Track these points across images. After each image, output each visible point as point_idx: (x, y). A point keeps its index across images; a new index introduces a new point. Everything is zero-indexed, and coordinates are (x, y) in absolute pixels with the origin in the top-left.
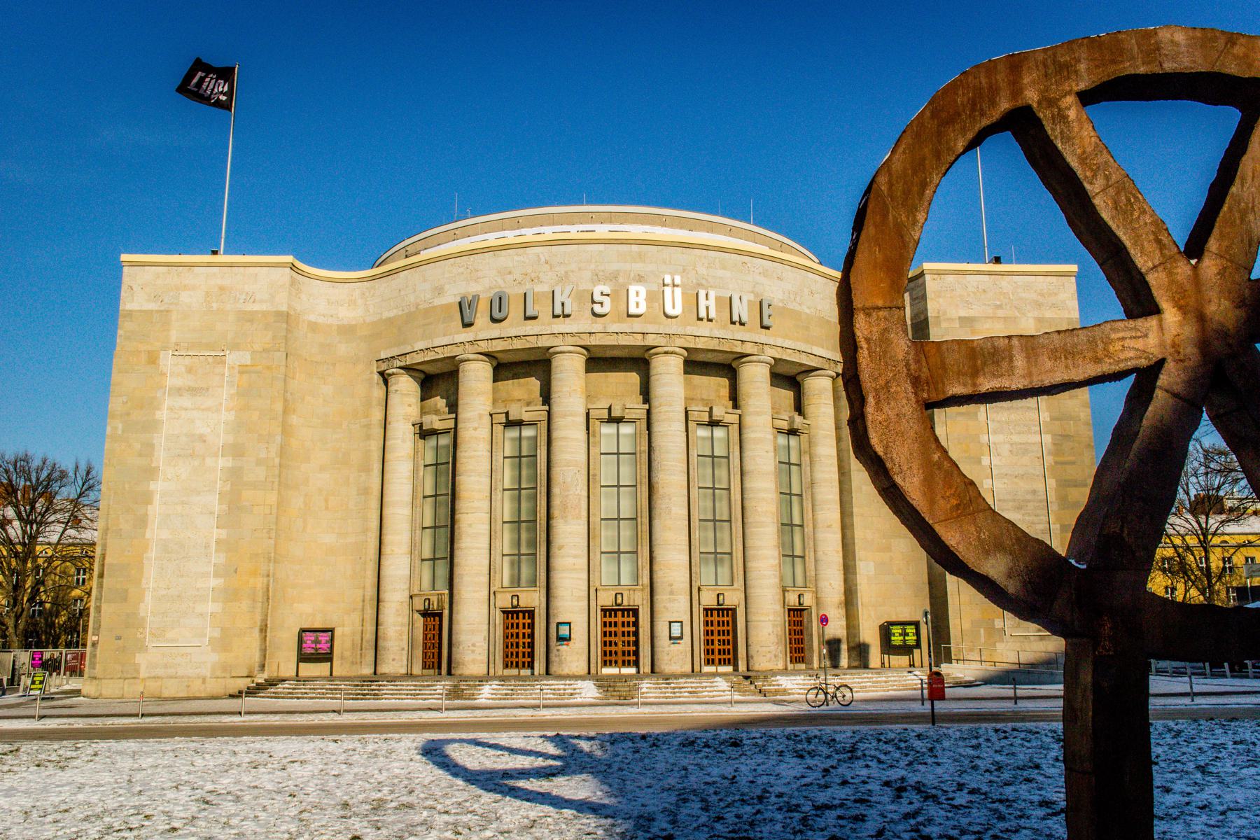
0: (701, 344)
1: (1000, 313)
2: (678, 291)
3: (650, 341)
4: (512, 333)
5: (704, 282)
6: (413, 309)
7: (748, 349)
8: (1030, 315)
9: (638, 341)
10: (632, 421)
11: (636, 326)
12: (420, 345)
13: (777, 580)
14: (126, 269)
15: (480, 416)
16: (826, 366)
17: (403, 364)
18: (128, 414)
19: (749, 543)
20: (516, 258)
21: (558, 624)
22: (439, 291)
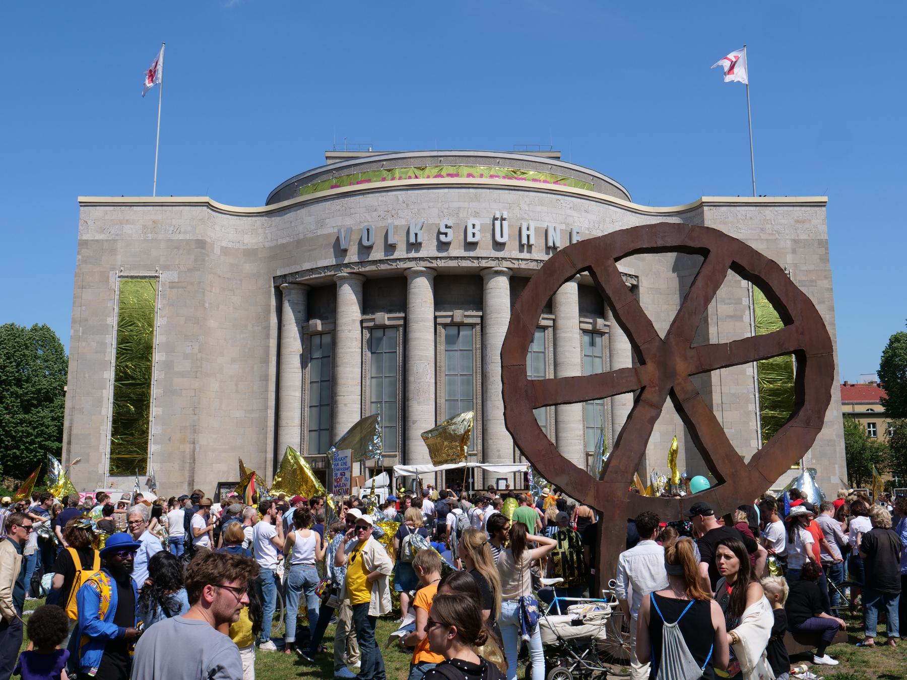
0: (523, 265)
1: (763, 236)
3: (484, 264)
5: (526, 216)
6: (301, 236)
9: (475, 264)
12: (307, 266)
13: (582, 447)
15: (354, 321)
17: (294, 280)
18: (87, 320)
19: (561, 418)
20: (380, 199)
22: (321, 223)
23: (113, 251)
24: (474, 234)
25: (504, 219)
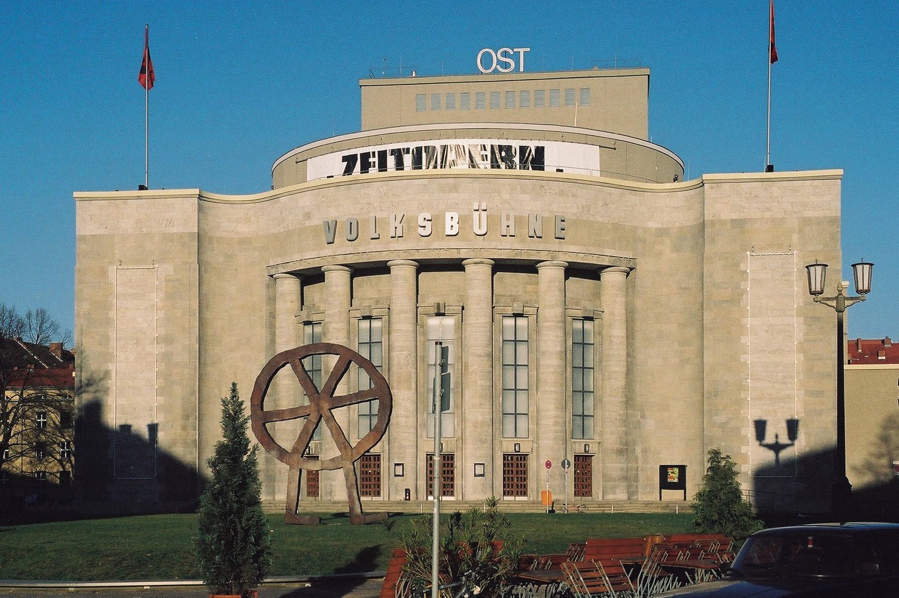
1: (768, 215)
4: (361, 250)
6: (291, 228)
9: (455, 255)
10: (452, 315)
11: (453, 243)
12: (296, 257)
14: (78, 203)
18: (89, 314)
22: (308, 216)
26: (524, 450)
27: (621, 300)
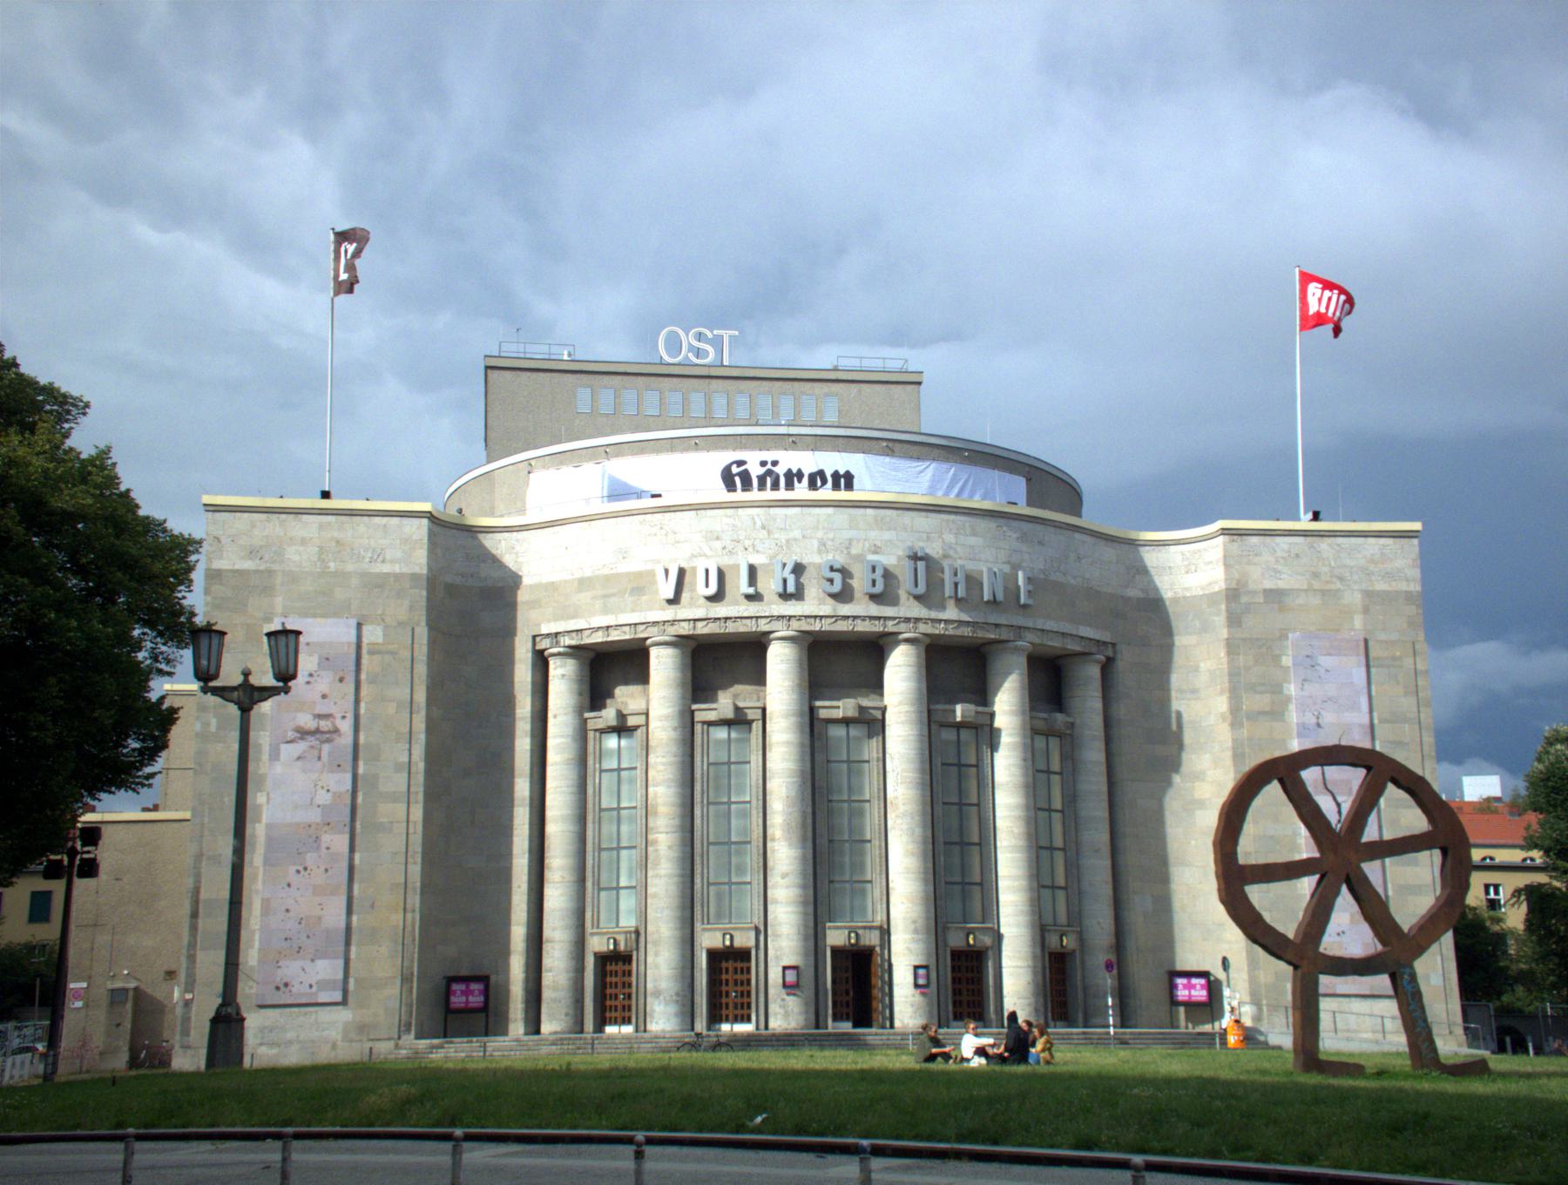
1: (1316, 585)
2: (921, 565)
5: (951, 552)
6: (588, 574)
7: (1004, 634)
8: (1356, 587)
9: (877, 627)
16: (1094, 649)
17: (573, 643)
20: (726, 520)
21: (785, 968)
23: (268, 590)
24: (874, 582)
25: (921, 559)
26: (987, 940)
27: (1098, 705)
